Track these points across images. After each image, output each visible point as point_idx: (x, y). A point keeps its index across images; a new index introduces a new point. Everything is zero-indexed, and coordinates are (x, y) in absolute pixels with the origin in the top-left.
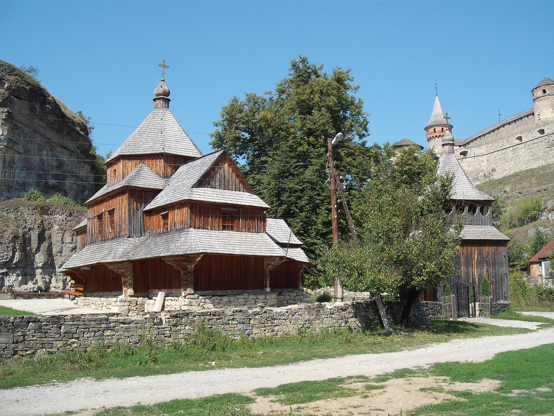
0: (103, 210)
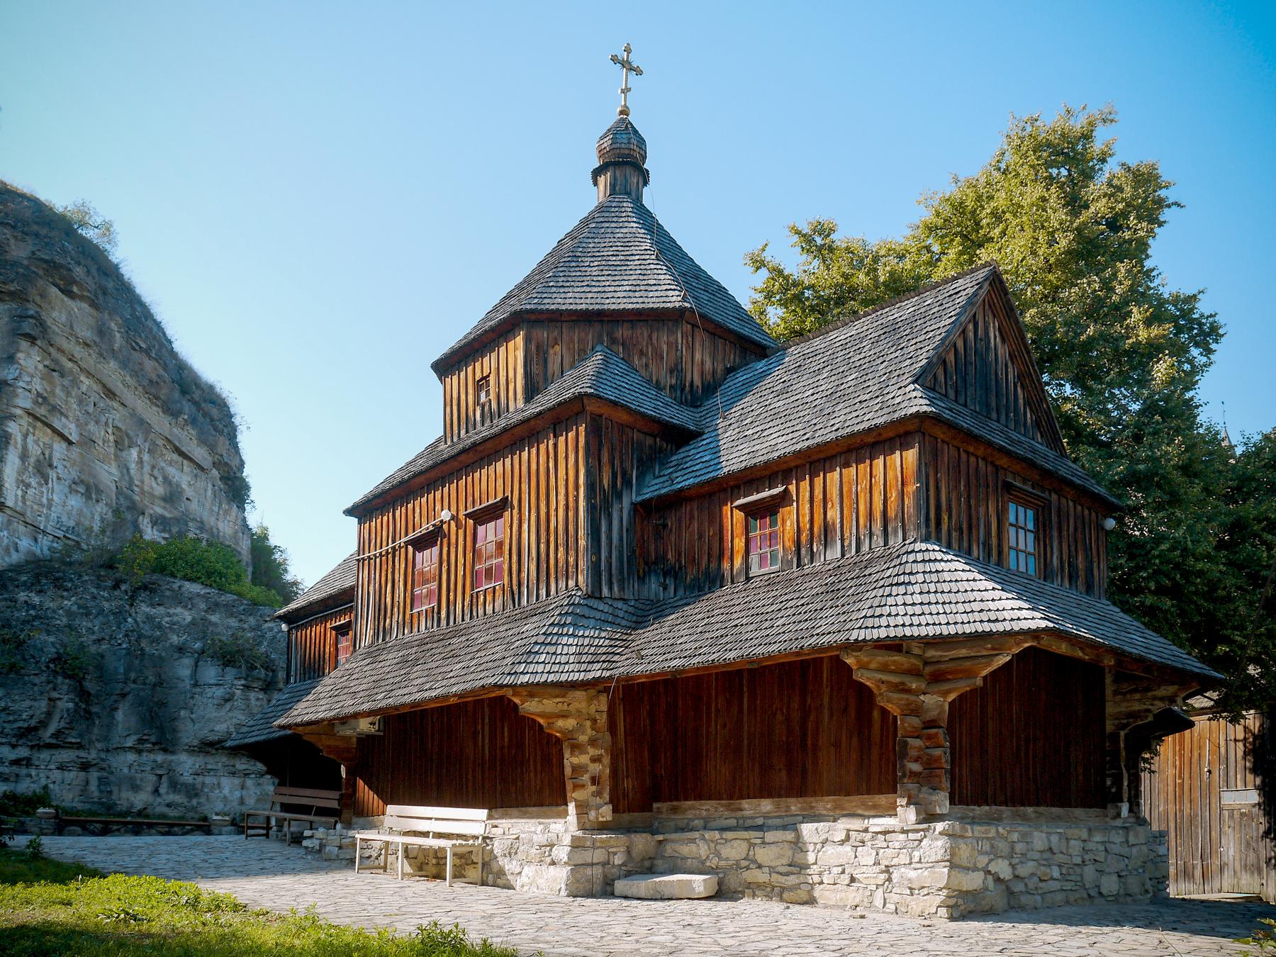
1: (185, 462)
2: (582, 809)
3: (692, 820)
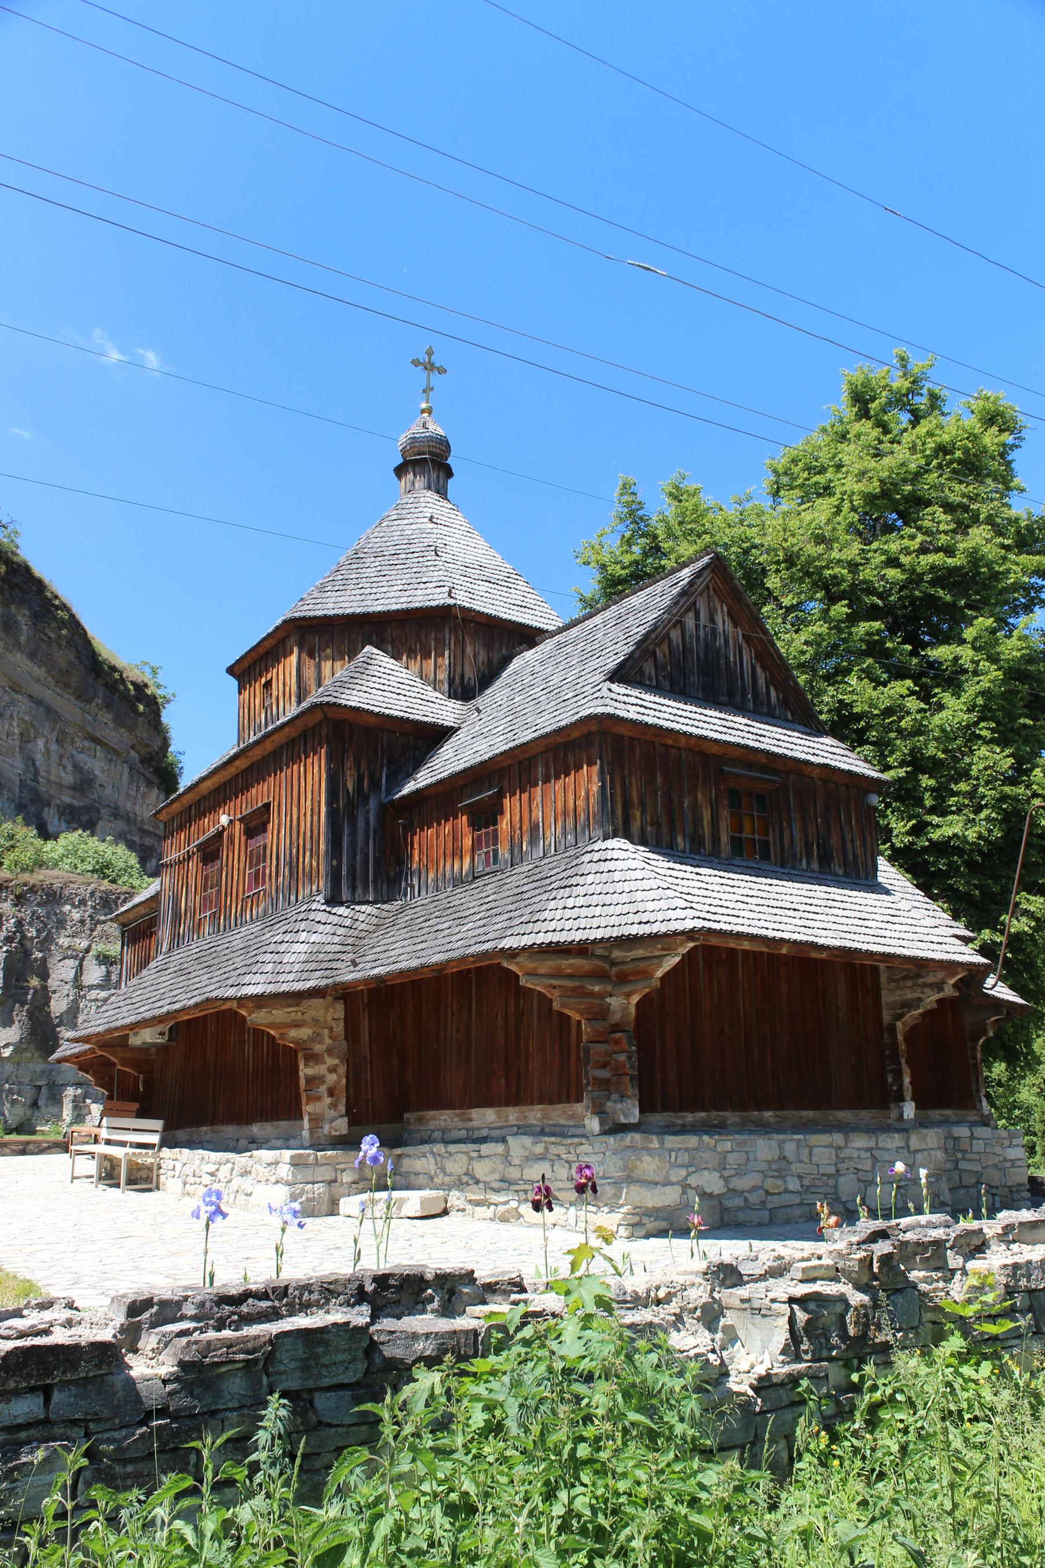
0: (224, 820)
1: (98, 748)
2: (316, 1120)
3: (433, 1131)
